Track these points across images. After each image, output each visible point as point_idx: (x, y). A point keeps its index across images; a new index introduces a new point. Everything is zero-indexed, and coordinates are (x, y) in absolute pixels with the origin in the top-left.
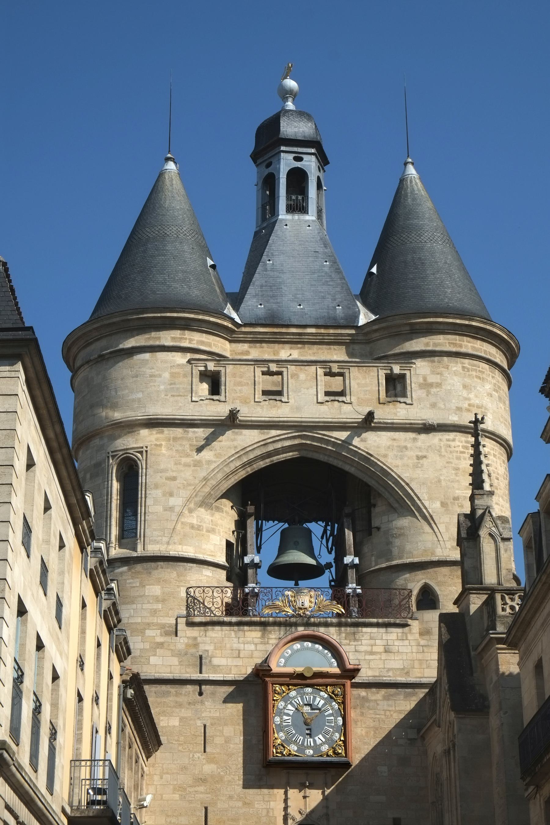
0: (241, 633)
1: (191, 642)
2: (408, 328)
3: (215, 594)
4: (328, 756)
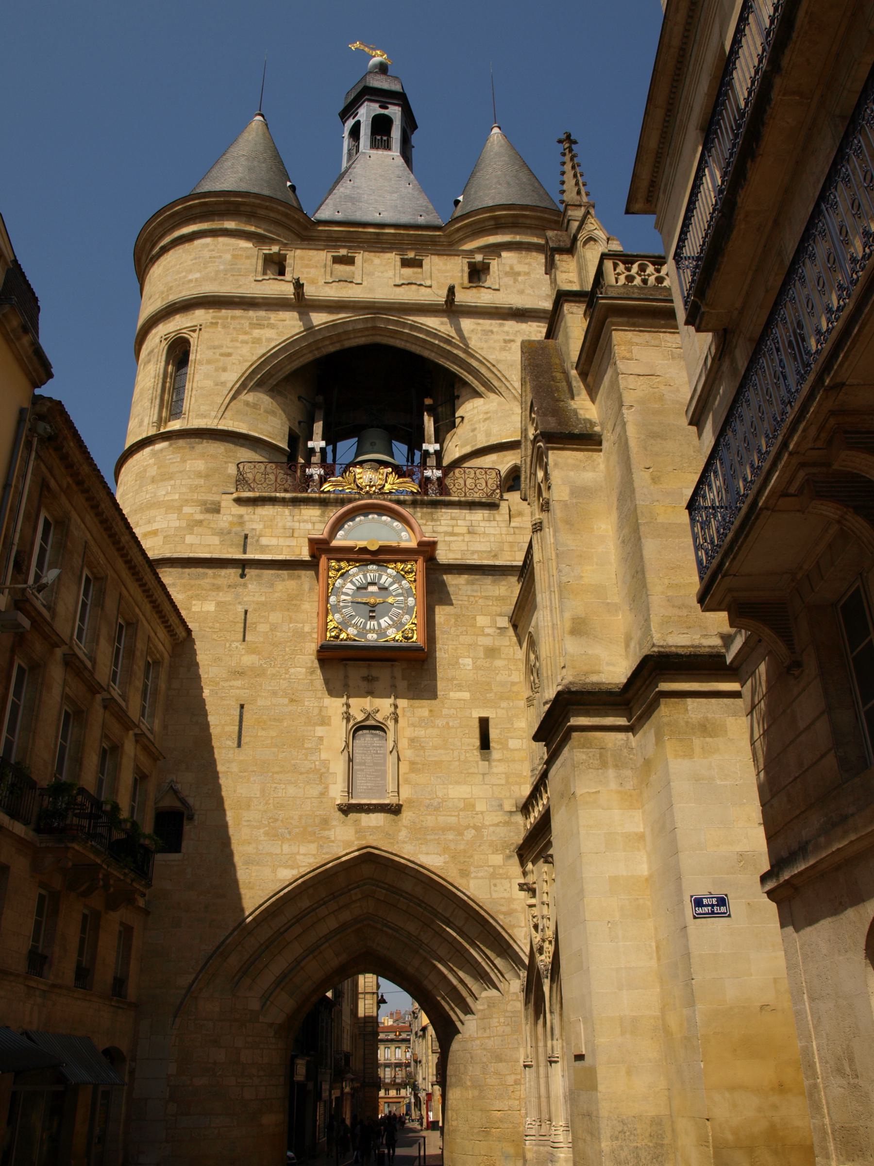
0: (296, 511)
1: (235, 520)
2: (492, 223)
3: (268, 470)
4: (397, 641)
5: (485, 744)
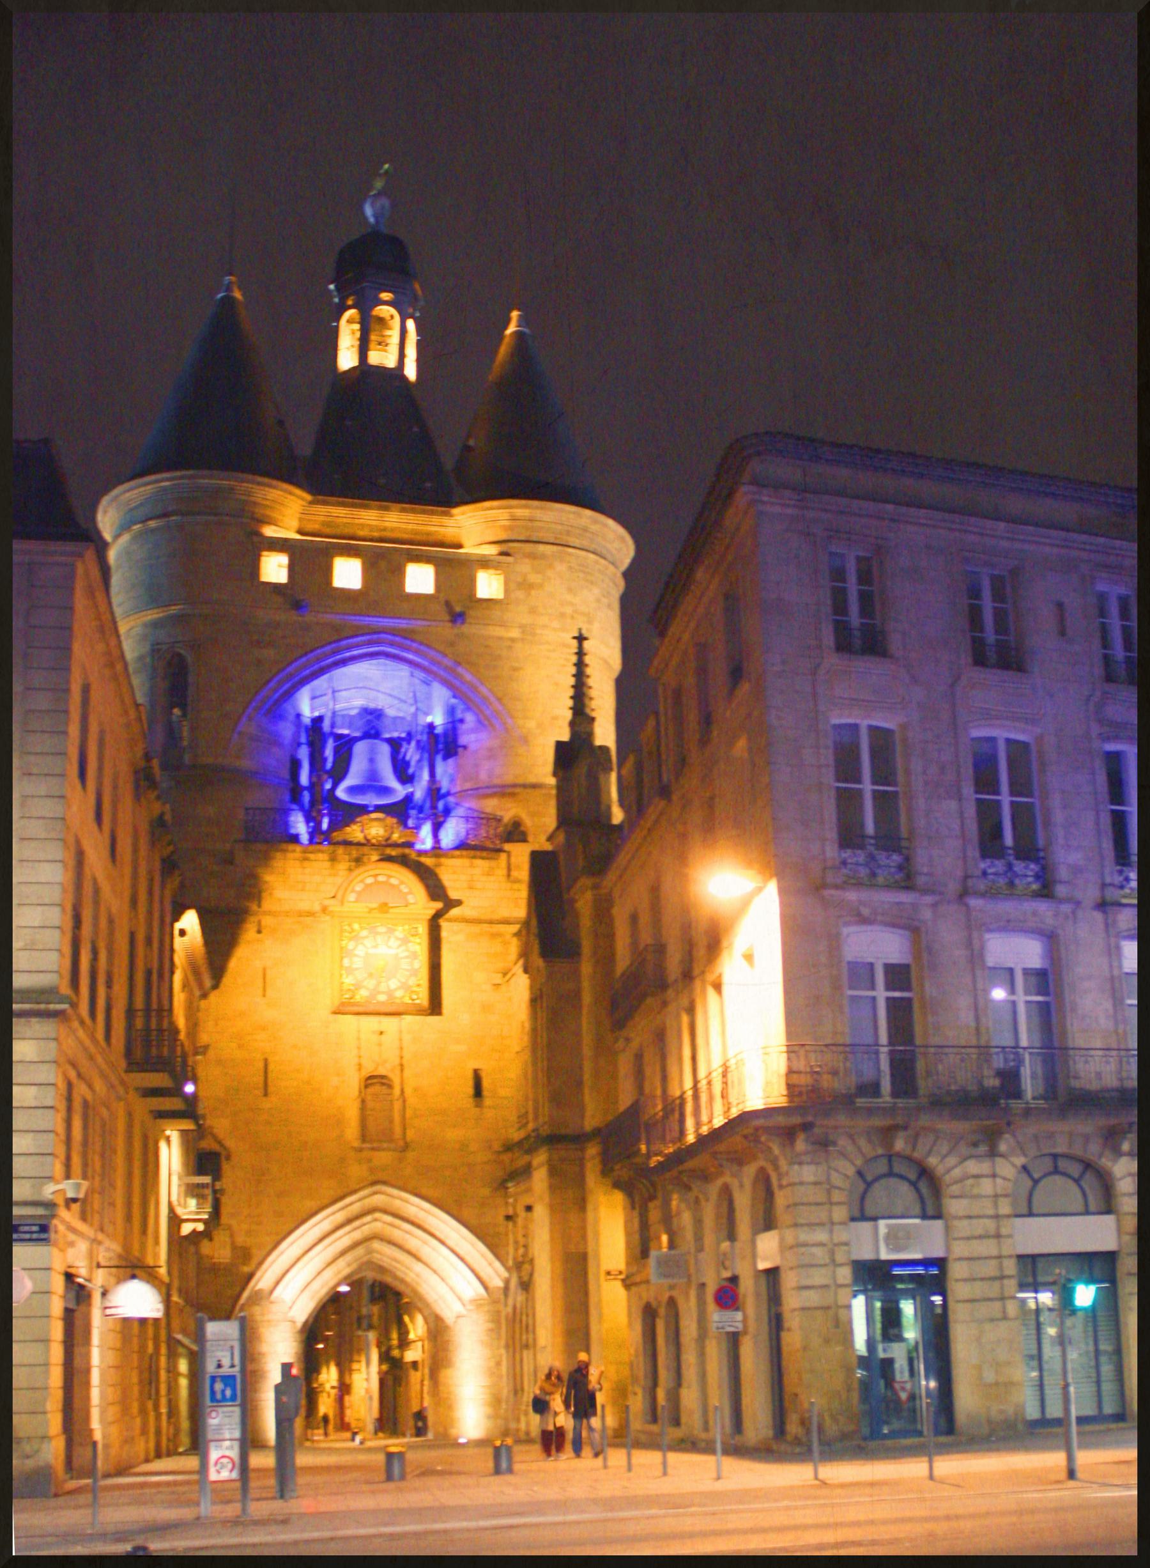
5: (478, 1091)
